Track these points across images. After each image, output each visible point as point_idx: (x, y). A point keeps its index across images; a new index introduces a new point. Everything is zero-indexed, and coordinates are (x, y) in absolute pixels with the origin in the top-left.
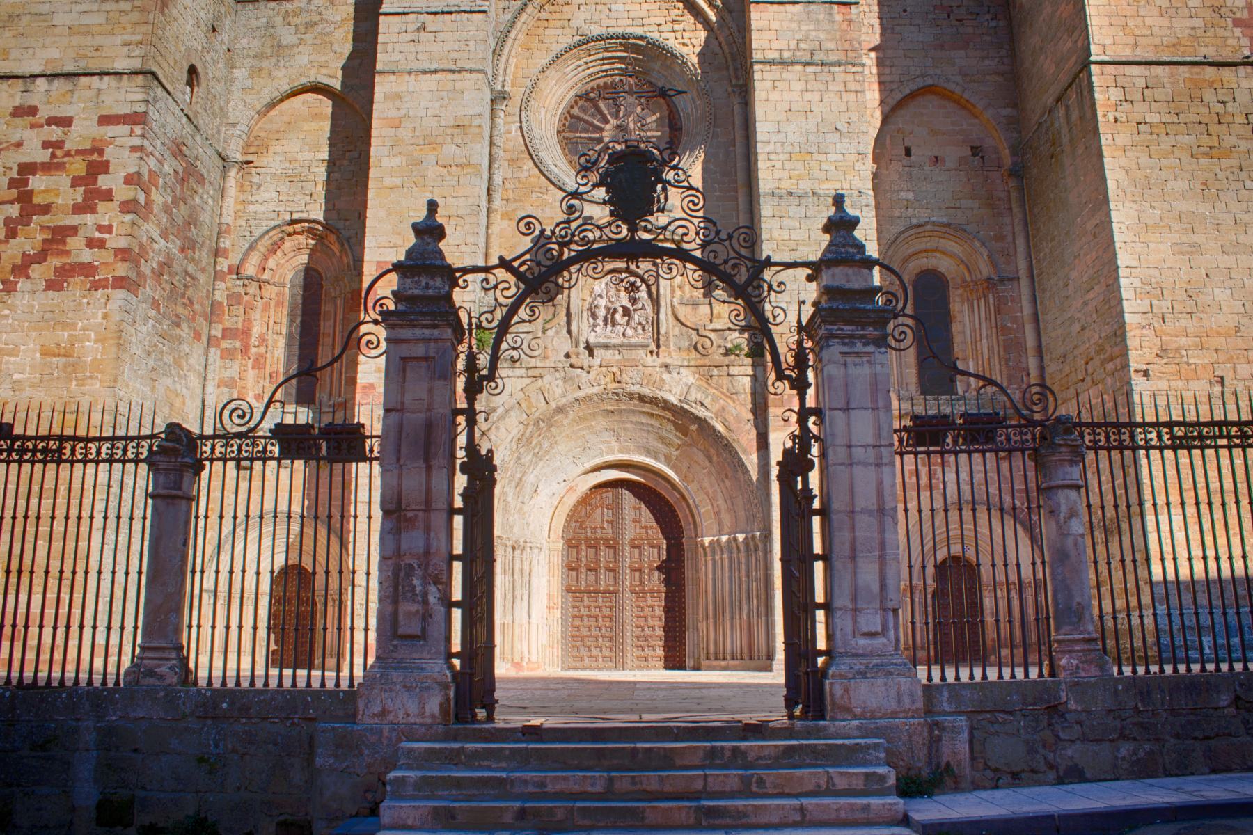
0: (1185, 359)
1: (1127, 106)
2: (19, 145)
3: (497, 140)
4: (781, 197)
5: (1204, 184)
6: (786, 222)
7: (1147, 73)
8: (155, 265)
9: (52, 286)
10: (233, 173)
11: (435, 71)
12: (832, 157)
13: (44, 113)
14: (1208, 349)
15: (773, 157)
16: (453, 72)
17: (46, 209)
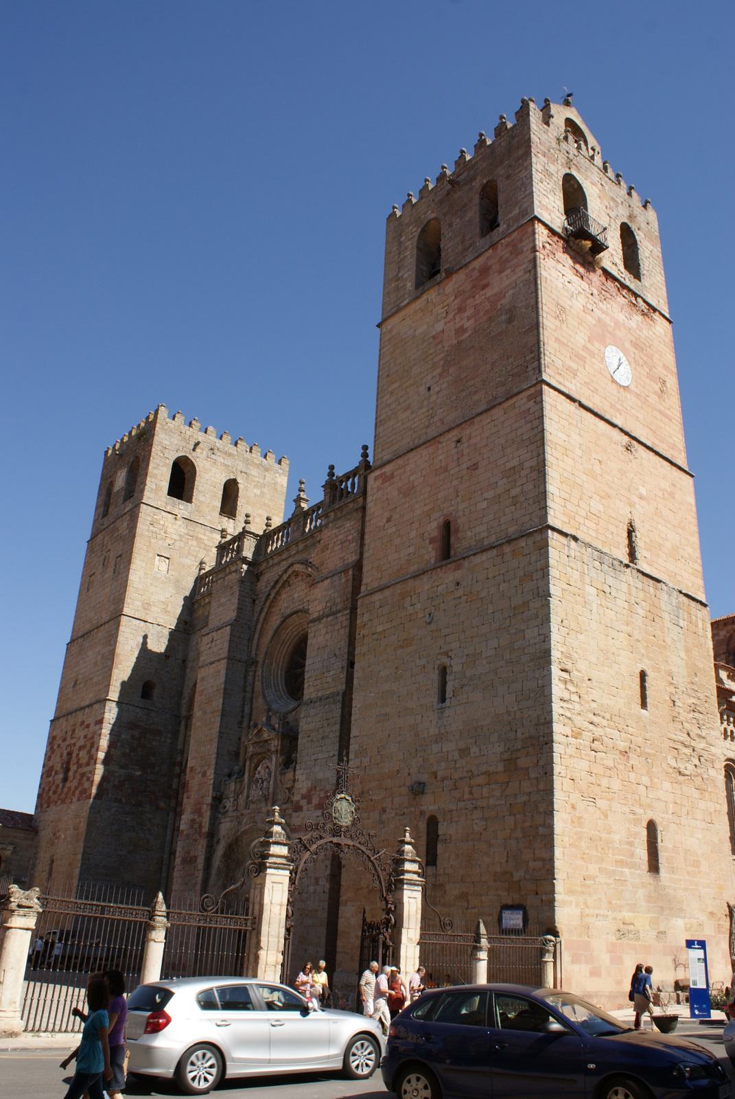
0: (370, 797)
1: (370, 623)
2: (79, 738)
3: (248, 689)
4: (308, 704)
5: (397, 668)
6: (309, 719)
7: (381, 597)
8: (116, 783)
9: (79, 800)
10: (183, 723)
11: (213, 663)
12: (332, 673)
13: (86, 723)
14: (382, 788)
15: (310, 680)
16: (218, 661)
17: (80, 766)
